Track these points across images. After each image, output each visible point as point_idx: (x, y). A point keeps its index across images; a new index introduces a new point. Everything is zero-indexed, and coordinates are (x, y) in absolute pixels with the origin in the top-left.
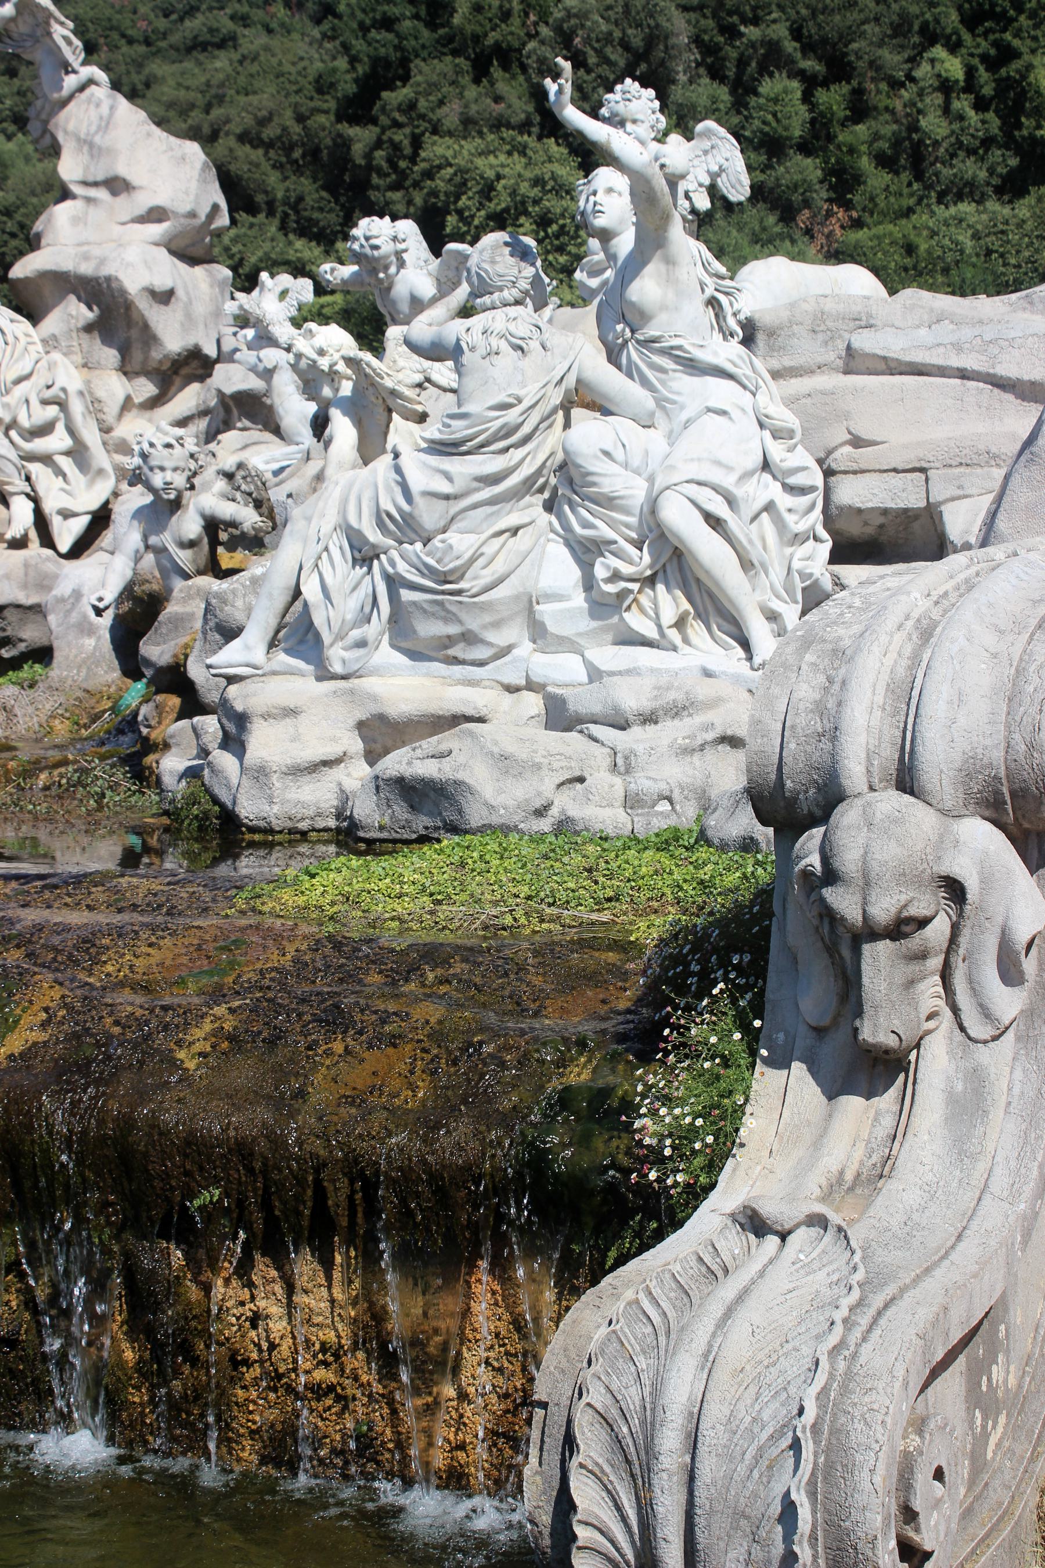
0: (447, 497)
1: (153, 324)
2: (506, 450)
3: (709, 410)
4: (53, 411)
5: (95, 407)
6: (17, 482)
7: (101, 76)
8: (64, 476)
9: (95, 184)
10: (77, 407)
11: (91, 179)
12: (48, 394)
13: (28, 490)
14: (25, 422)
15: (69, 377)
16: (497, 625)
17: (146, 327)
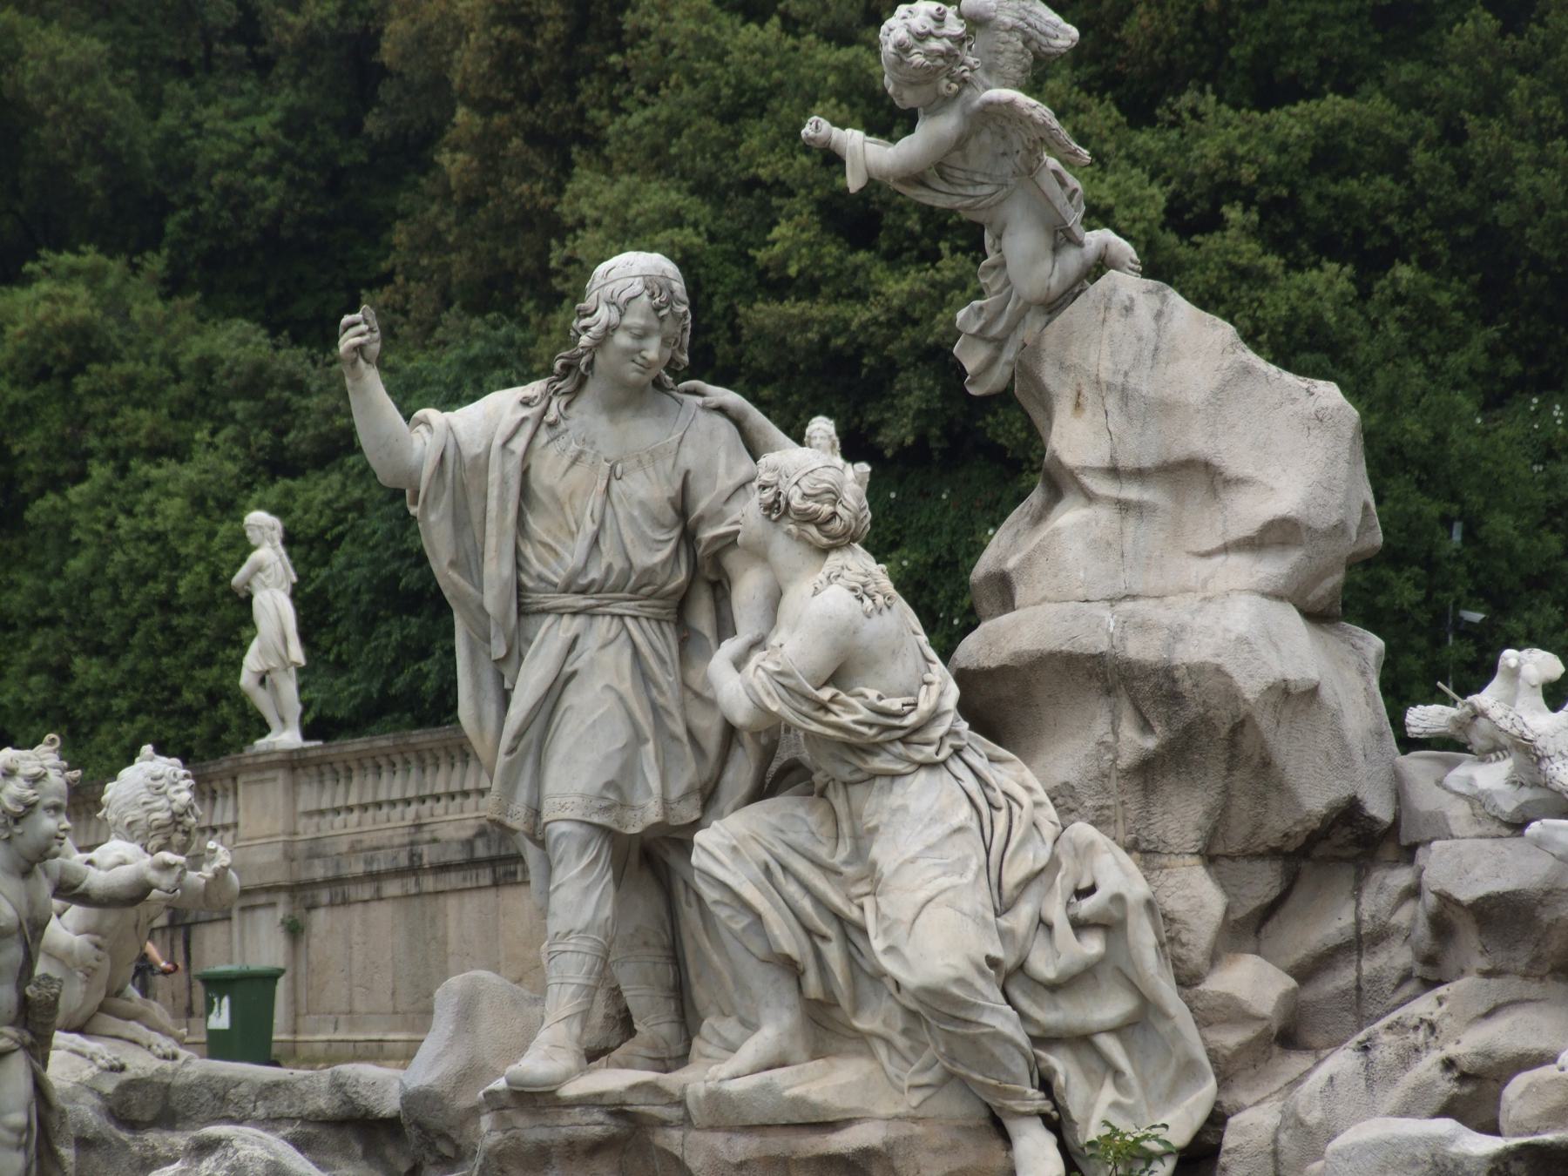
1: (1279, 760)
4: (1093, 945)
5: (1168, 925)
6: (1031, 1091)
7: (1124, 248)
8: (1117, 1073)
9: (1139, 475)
10: (1143, 936)
11: (1127, 461)
12: (1086, 906)
13: (1047, 1107)
14: (1045, 966)
15: (1116, 873)
17: (1266, 763)
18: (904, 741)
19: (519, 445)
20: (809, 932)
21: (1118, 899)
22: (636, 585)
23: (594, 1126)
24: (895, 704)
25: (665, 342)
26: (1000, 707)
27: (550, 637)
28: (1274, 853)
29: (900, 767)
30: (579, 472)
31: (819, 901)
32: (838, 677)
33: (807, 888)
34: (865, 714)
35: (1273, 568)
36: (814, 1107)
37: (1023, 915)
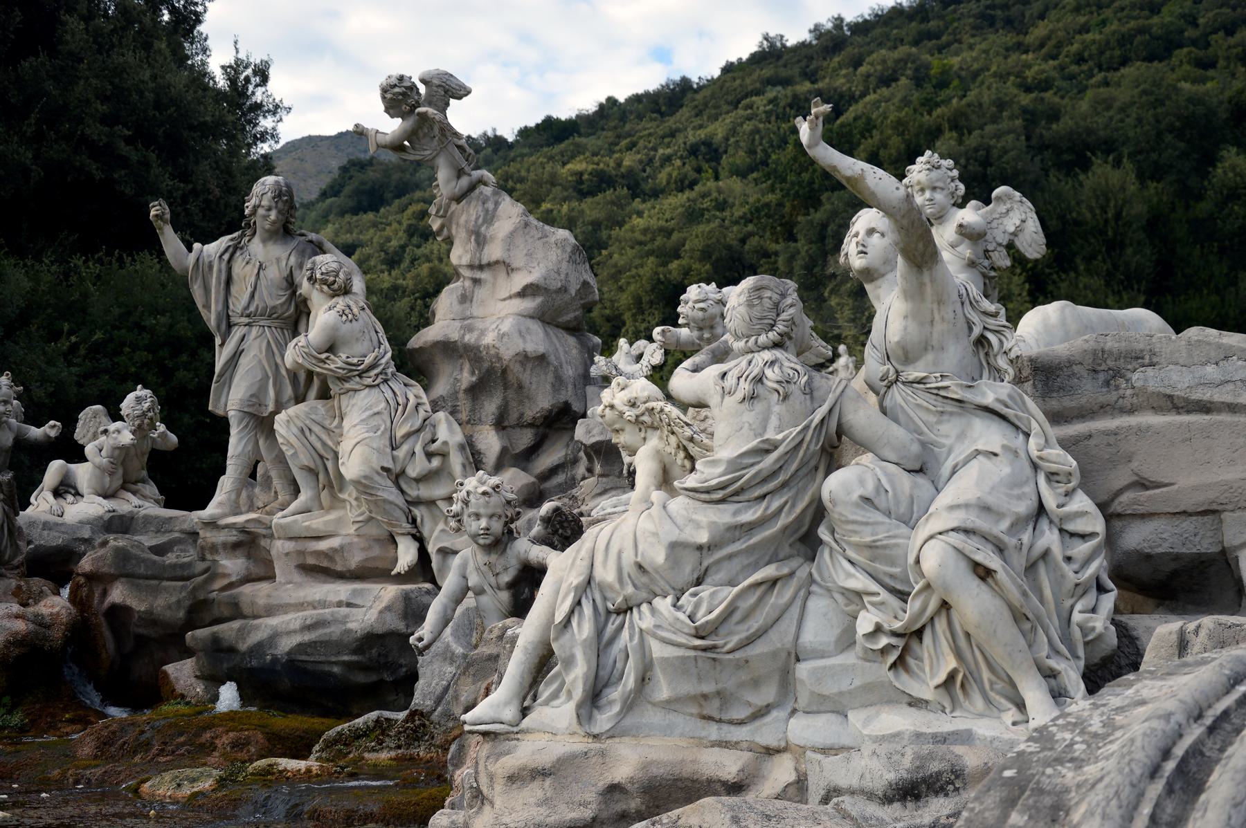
0: (700, 548)
2: (764, 496)
3: (978, 452)
16: (756, 683)
17: (520, 387)
18: (360, 376)
19: (226, 257)
20: (321, 457)
21: (445, 443)
22: (270, 314)
23: (232, 537)
24: (355, 361)
25: (279, 212)
26: (414, 366)
27: (237, 333)
28: (531, 425)
29: (357, 387)
30: (249, 266)
31: (324, 444)
32: (331, 349)
33: (320, 439)
34: (340, 364)
35: (529, 304)
36: (314, 530)
37: (401, 452)
